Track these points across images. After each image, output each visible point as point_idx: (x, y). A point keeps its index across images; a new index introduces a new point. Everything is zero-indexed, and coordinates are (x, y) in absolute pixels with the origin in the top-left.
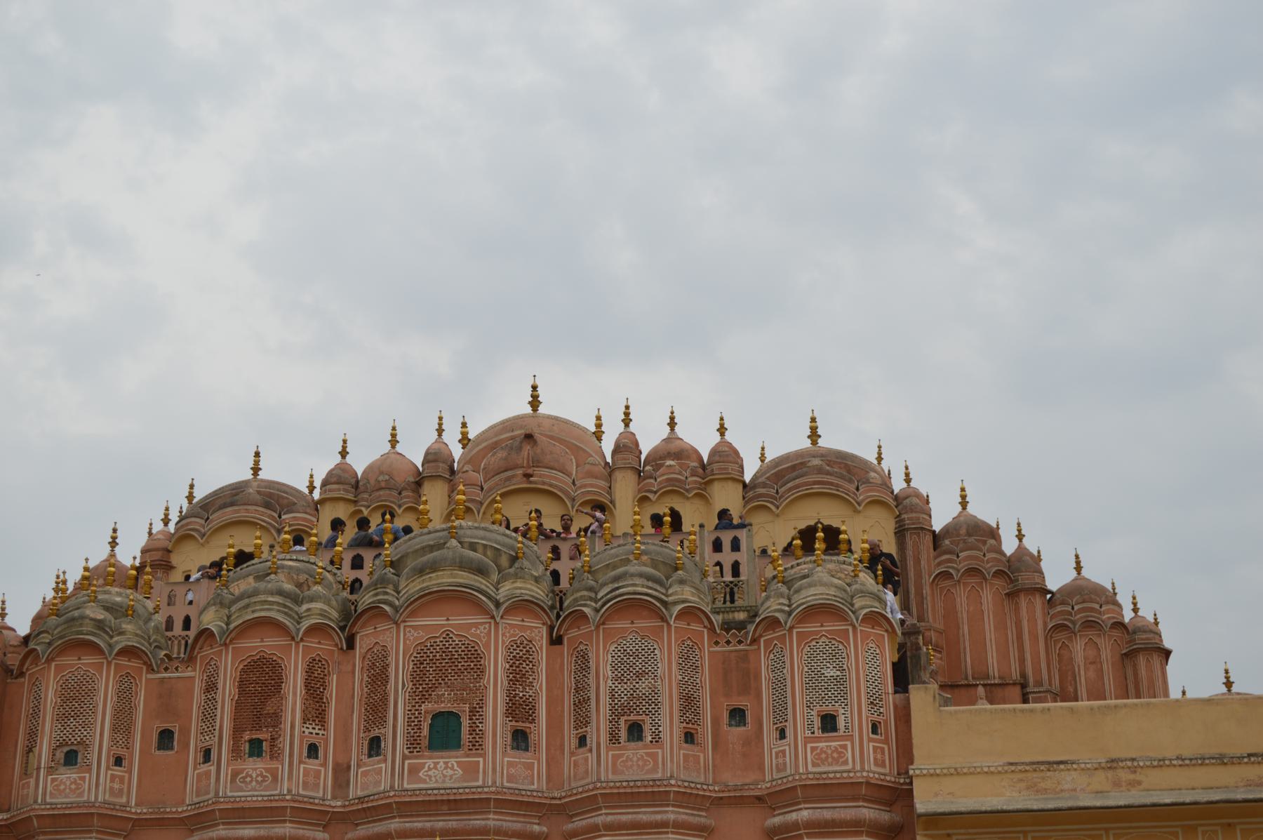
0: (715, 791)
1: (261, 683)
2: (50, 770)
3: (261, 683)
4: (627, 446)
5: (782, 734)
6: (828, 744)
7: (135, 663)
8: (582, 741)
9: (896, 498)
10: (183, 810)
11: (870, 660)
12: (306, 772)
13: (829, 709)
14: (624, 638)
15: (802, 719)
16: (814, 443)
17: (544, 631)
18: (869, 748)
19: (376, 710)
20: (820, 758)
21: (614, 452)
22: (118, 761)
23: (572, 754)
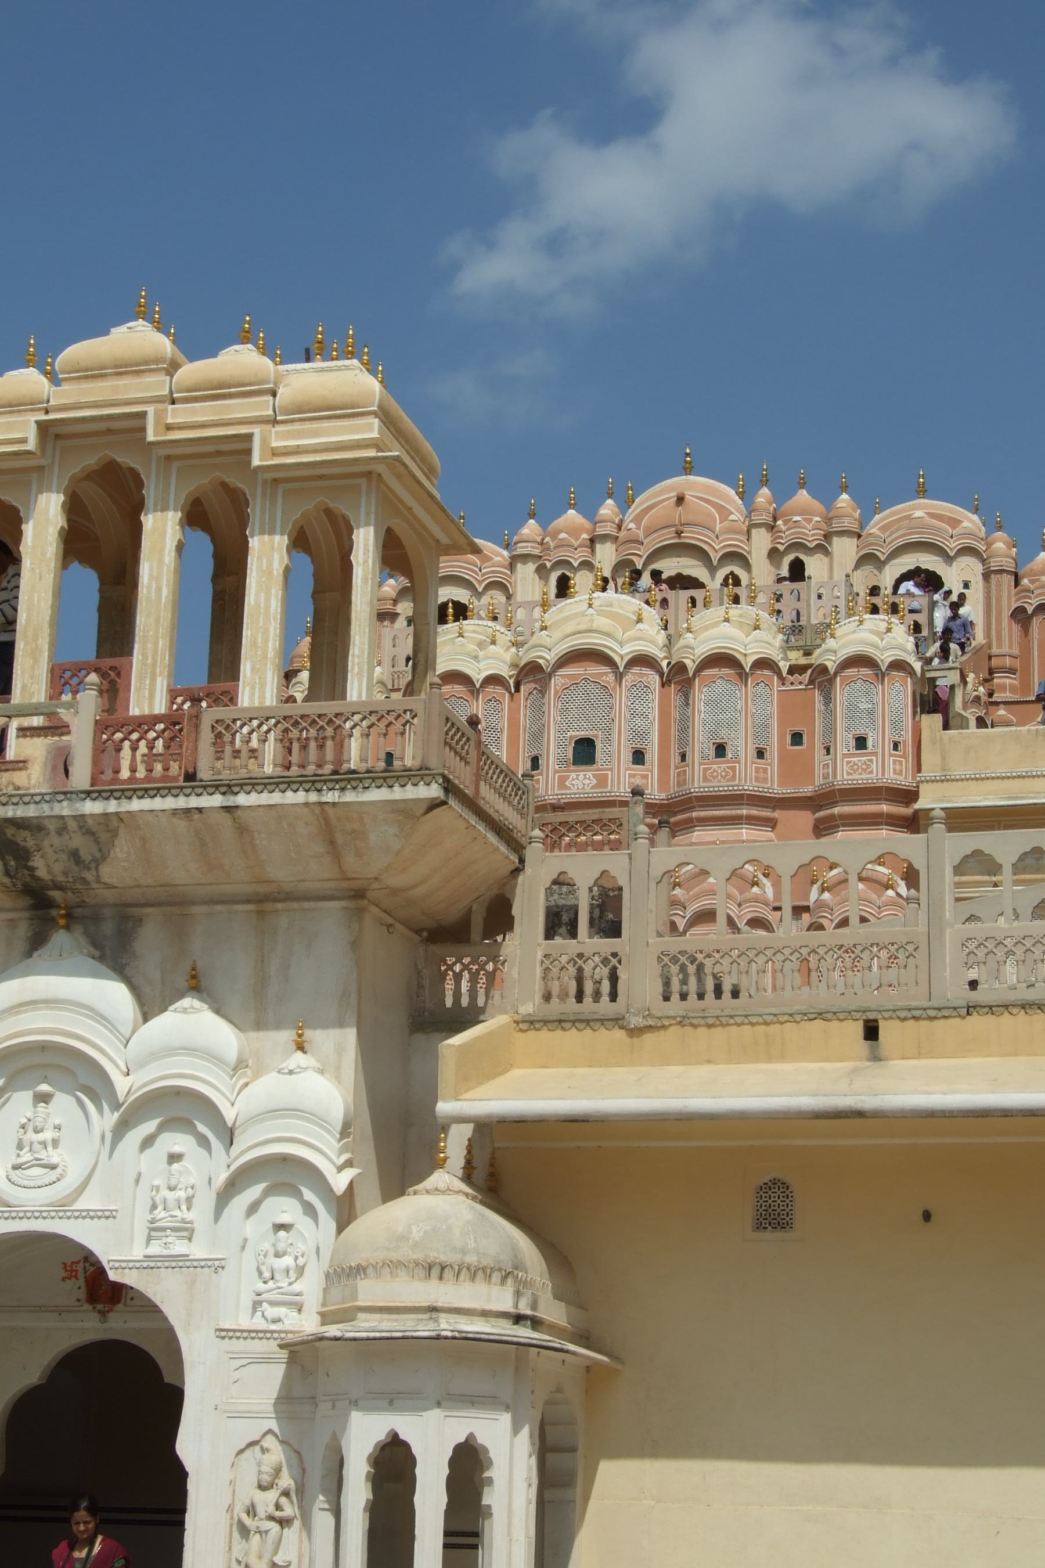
6: (860, 759)
8: (683, 757)
13: (860, 732)
14: (714, 682)
15: (844, 741)
17: (657, 678)
18: (890, 761)
19: (537, 736)
20: (854, 768)
23: (676, 768)
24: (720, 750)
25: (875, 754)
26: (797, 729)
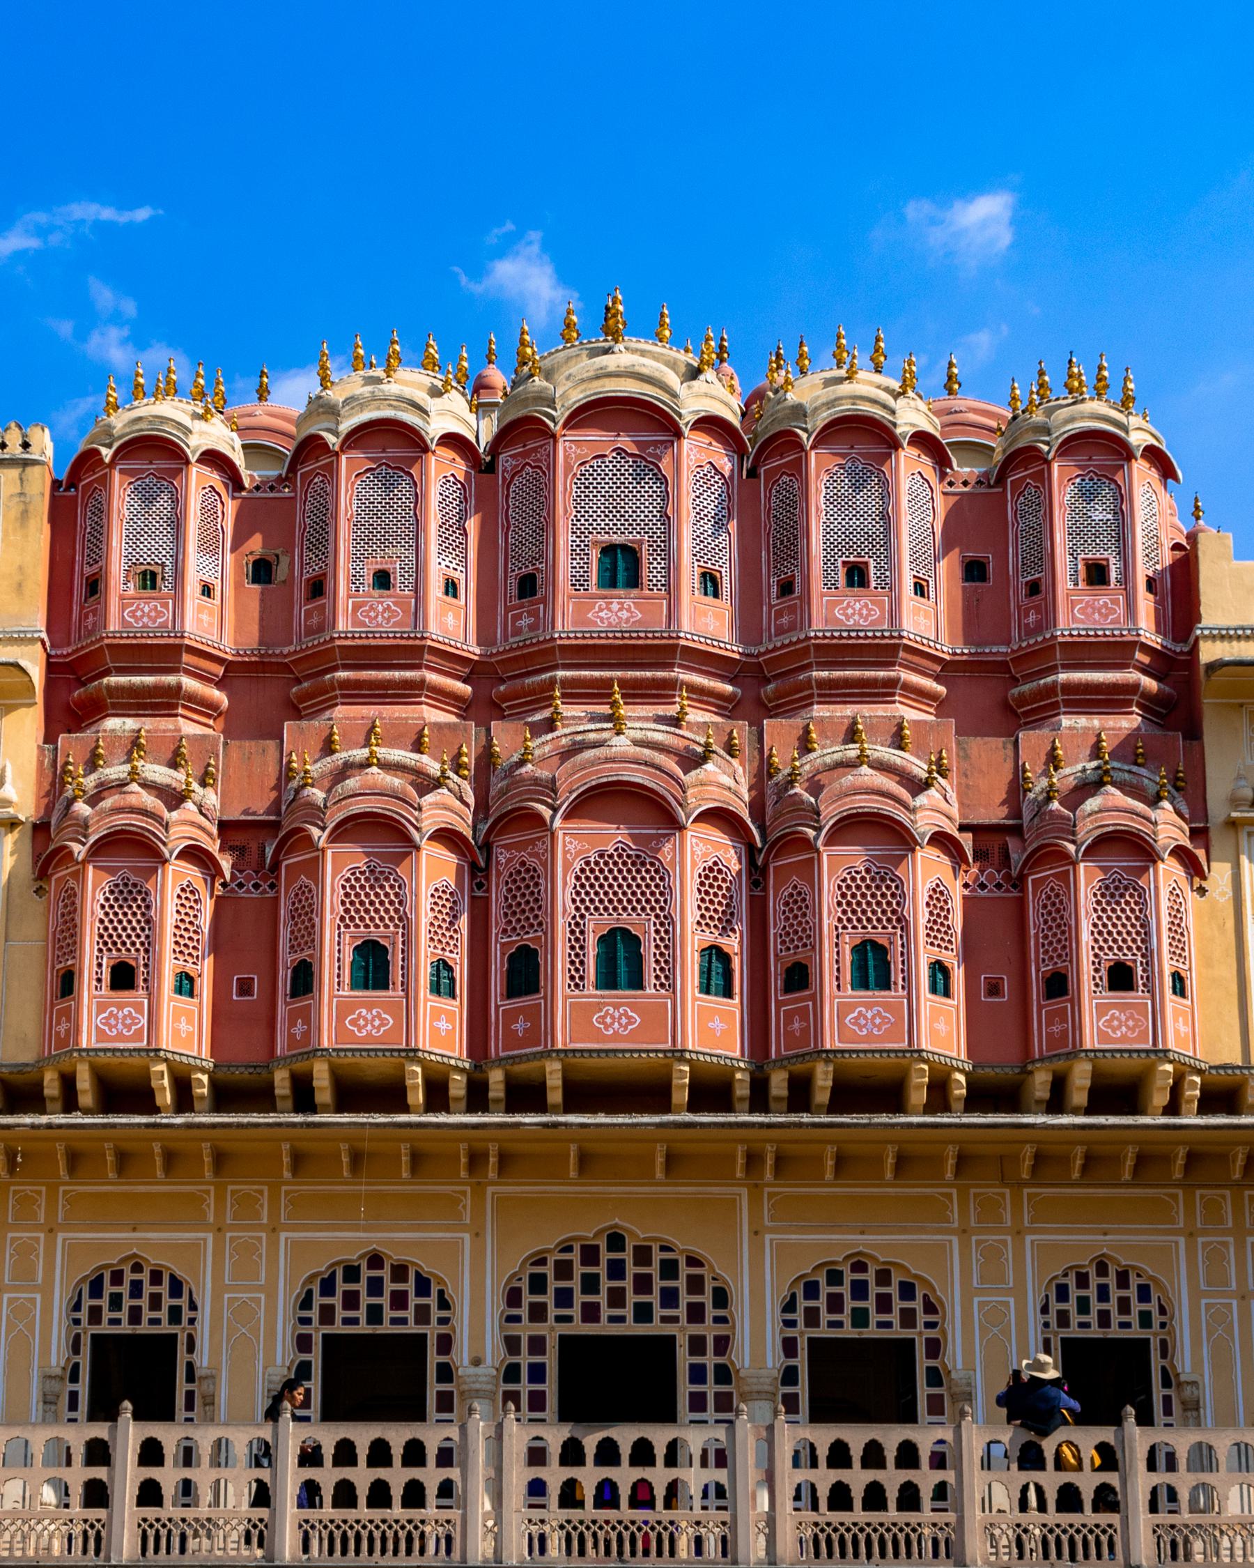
24: (857, 575)
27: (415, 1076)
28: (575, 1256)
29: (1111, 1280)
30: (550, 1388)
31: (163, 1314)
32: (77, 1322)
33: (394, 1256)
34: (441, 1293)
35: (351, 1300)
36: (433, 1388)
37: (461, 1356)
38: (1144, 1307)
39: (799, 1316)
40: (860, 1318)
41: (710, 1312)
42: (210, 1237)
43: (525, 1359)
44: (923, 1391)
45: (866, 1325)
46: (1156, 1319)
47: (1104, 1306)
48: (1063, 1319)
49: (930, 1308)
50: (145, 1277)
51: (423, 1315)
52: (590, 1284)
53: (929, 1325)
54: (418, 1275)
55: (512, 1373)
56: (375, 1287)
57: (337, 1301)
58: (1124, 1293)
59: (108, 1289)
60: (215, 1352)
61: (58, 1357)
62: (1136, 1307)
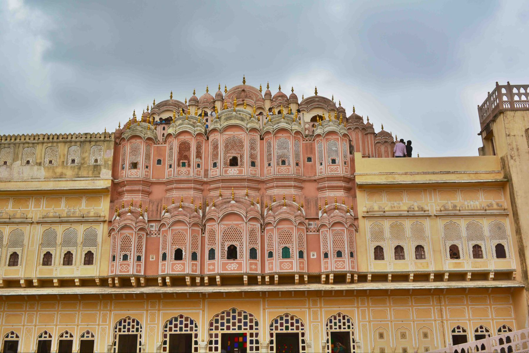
0: (304, 178)
1: (184, 148)
2: (129, 169)
3: (184, 148)
4: (268, 94)
5: (321, 164)
6: (334, 167)
7: (151, 142)
8: (269, 165)
9: (337, 109)
10: (165, 180)
11: (342, 147)
12: (197, 171)
13: (334, 157)
15: (327, 161)
16: (316, 95)
17: (259, 136)
19: (215, 155)
20: (332, 170)
21: (265, 95)
22: (147, 167)
23: (267, 168)
25: (339, 165)
26: (309, 156)
27: (188, 279)
28: (225, 315)
29: (341, 318)
30: (219, 346)
31: (135, 330)
32: (116, 332)
33: (185, 316)
34: (196, 324)
35: (176, 326)
36: (193, 346)
37: (199, 339)
38: (349, 324)
39: (274, 328)
40: (287, 328)
41: (254, 327)
42: (145, 312)
43: (214, 339)
44: (301, 345)
45: (288, 330)
46: (351, 327)
47: (340, 324)
48: (331, 327)
49: (302, 325)
50: (131, 321)
51: (191, 329)
52: (228, 321)
53: (302, 329)
54: (191, 320)
55: (211, 342)
56: (181, 323)
57: (173, 326)
58: (344, 321)
59: (123, 324)
60: (146, 340)
61: (111, 341)
62: (347, 324)
